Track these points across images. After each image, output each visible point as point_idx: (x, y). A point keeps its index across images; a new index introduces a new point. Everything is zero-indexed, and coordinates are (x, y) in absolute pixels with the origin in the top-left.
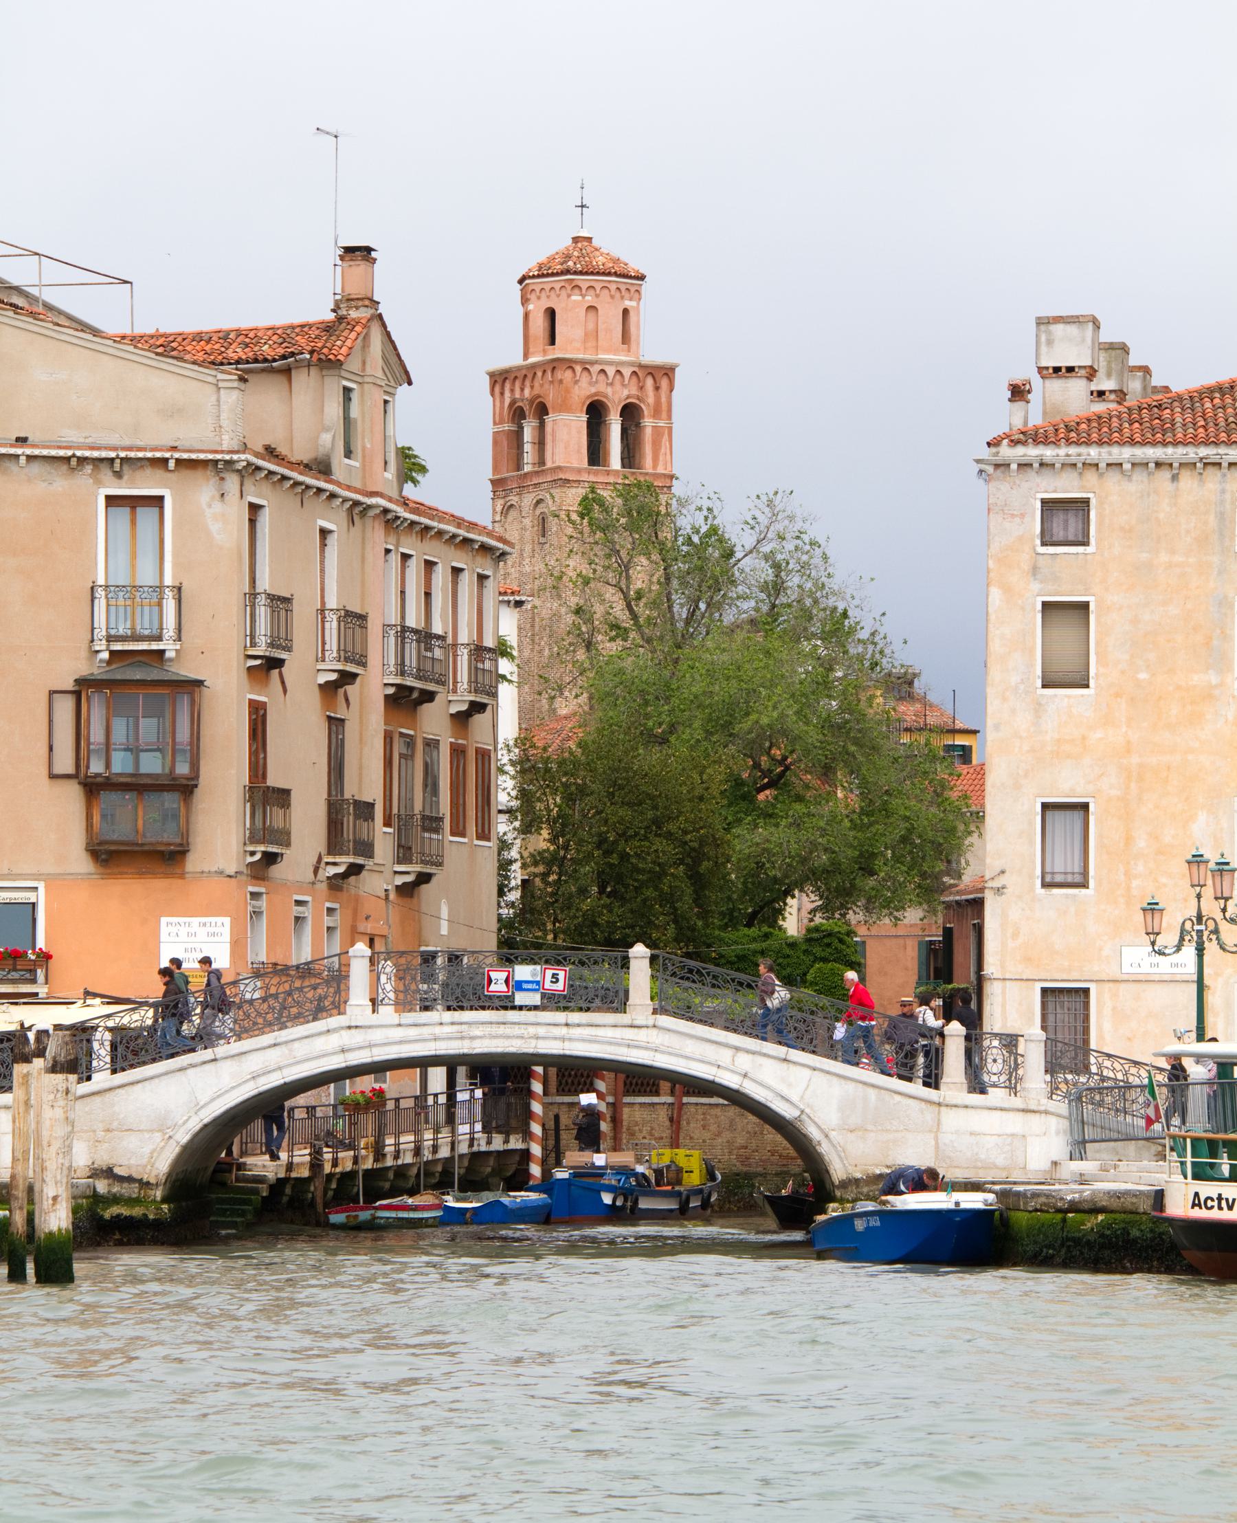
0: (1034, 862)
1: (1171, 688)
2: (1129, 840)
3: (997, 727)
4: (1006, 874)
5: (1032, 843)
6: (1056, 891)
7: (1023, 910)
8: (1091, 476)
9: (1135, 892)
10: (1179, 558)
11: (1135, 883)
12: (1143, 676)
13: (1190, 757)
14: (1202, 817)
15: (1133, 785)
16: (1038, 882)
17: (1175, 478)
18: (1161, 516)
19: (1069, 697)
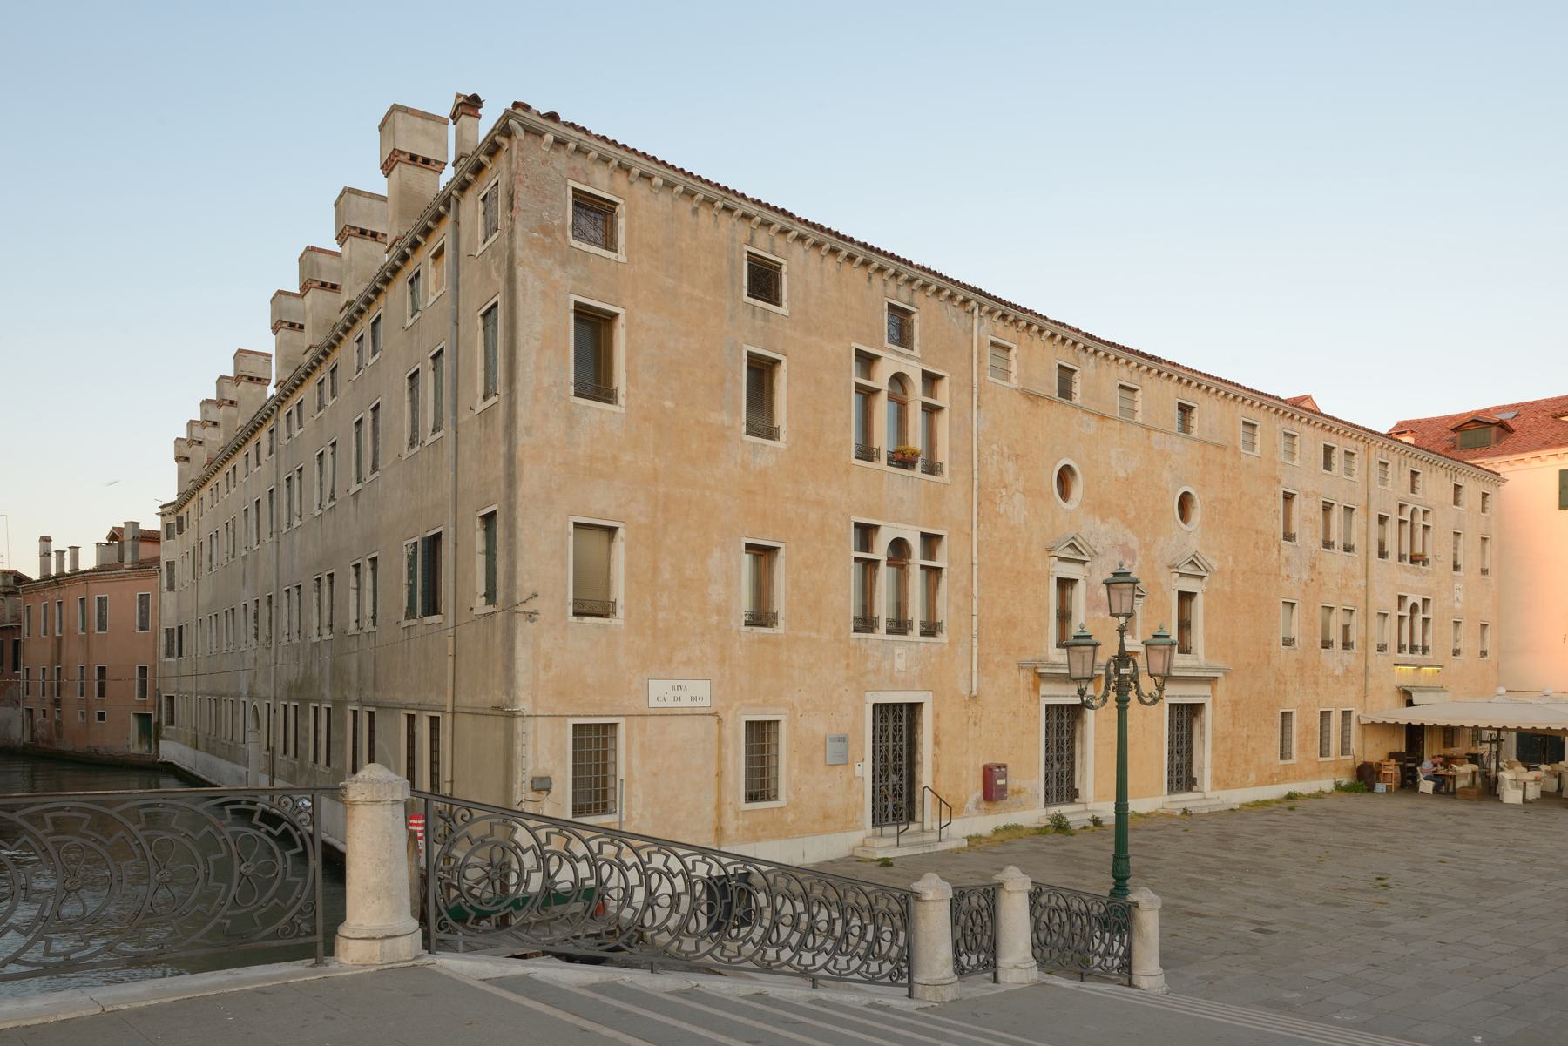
0: (566, 586)
1: (692, 422)
2: (655, 570)
3: (528, 430)
4: (538, 598)
5: (564, 565)
6: (587, 620)
7: (555, 639)
8: (621, 179)
9: (660, 625)
10: (698, 293)
11: (661, 615)
12: (668, 404)
13: (707, 493)
14: (717, 554)
15: (659, 515)
16: (570, 609)
17: (695, 211)
18: (684, 245)
19: (601, 411)
